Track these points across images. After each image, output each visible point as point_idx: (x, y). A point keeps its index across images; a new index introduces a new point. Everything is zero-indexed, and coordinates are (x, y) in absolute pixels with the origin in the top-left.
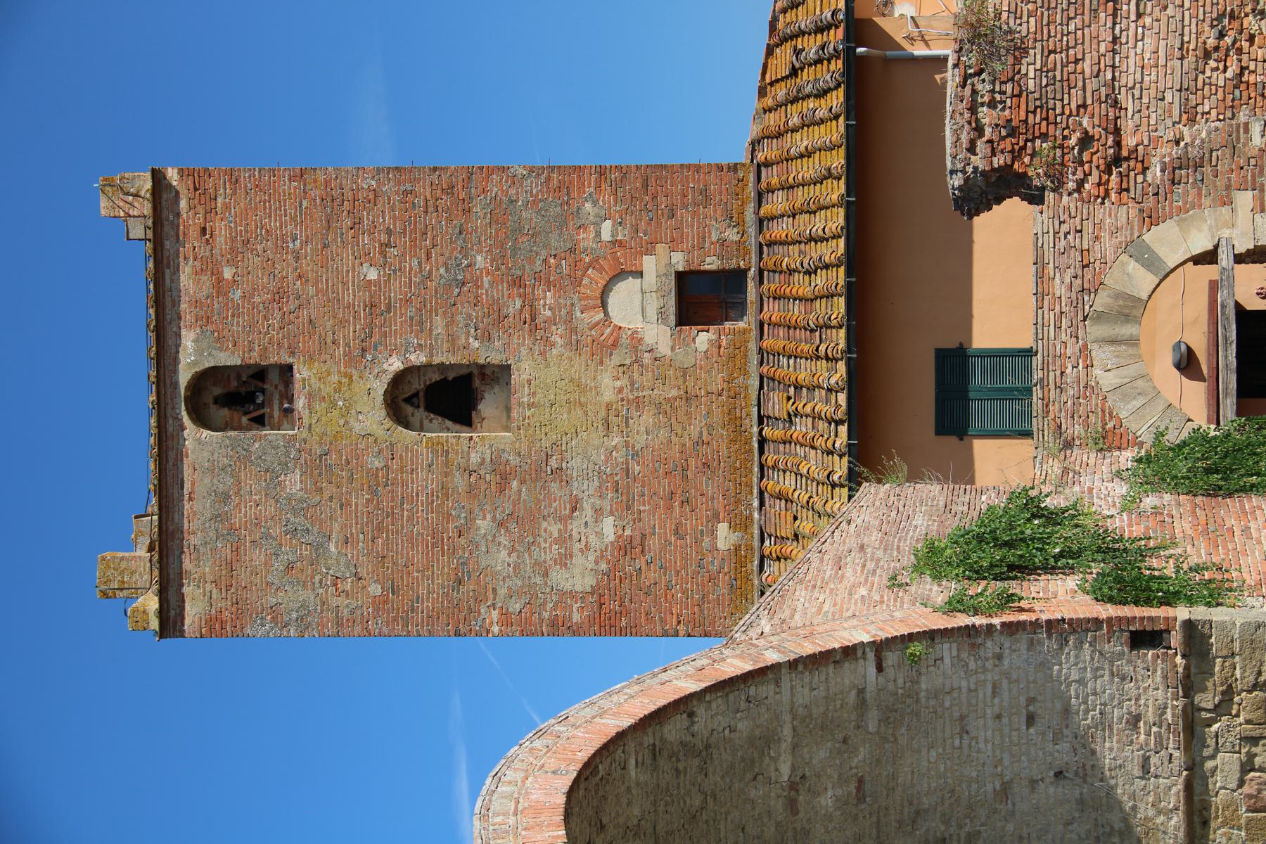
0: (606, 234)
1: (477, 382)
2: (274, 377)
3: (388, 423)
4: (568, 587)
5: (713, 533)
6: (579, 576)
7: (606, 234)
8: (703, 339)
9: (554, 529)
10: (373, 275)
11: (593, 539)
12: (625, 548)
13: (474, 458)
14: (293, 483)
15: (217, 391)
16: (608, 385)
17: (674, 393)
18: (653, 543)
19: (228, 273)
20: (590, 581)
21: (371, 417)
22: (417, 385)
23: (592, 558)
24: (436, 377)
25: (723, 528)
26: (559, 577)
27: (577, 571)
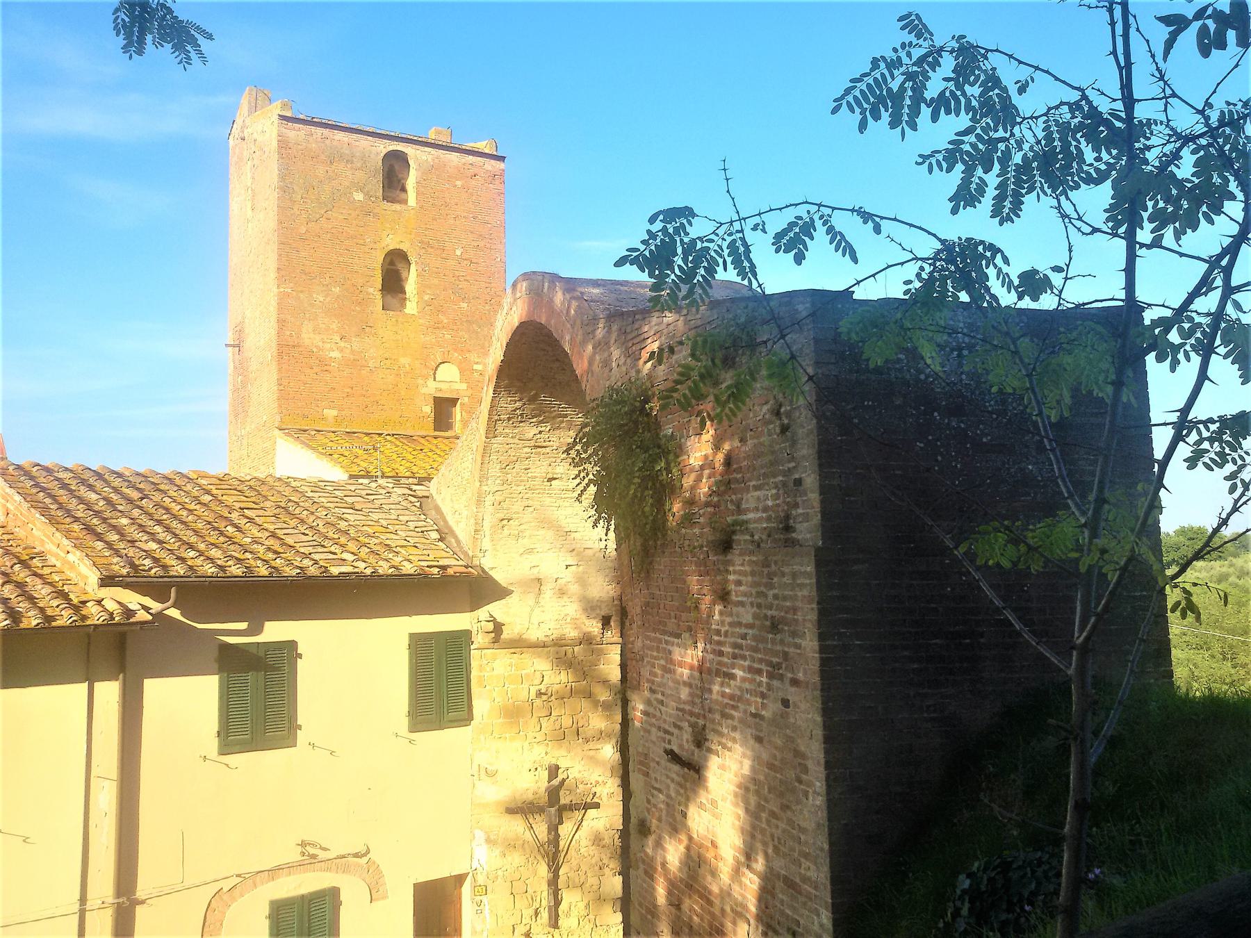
0: (475, 367)
1: (401, 295)
2: (403, 195)
3: (387, 250)
4: (304, 330)
5: (333, 408)
6: (308, 337)
7: (475, 367)
8: (428, 409)
9: (334, 326)
10: (458, 253)
11: (328, 346)
12: (324, 364)
13: (371, 290)
14: (359, 196)
15: (397, 167)
16: (404, 361)
17: (403, 393)
18: (328, 377)
19: (459, 183)
20: (307, 342)
21: (391, 242)
22: (400, 266)
23: (320, 344)
24: (404, 275)
25: (334, 413)
26: (307, 328)
27: (312, 335)
